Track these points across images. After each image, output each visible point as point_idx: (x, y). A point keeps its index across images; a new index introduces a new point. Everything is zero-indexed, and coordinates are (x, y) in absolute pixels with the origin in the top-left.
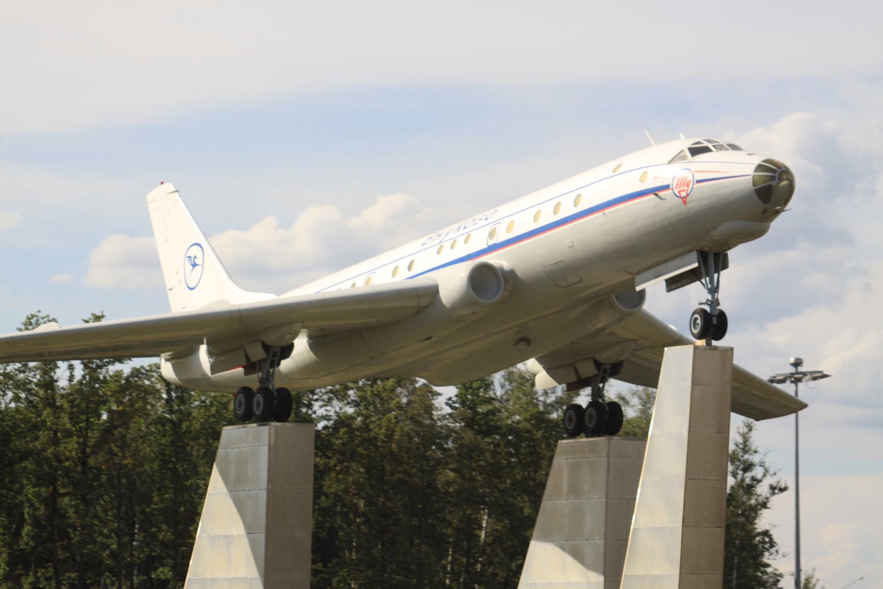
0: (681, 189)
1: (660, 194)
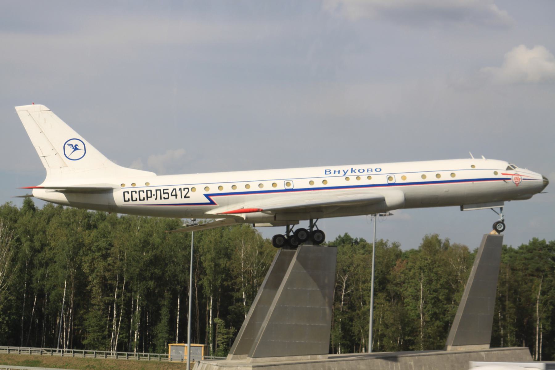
0: (516, 181)
1: (507, 181)
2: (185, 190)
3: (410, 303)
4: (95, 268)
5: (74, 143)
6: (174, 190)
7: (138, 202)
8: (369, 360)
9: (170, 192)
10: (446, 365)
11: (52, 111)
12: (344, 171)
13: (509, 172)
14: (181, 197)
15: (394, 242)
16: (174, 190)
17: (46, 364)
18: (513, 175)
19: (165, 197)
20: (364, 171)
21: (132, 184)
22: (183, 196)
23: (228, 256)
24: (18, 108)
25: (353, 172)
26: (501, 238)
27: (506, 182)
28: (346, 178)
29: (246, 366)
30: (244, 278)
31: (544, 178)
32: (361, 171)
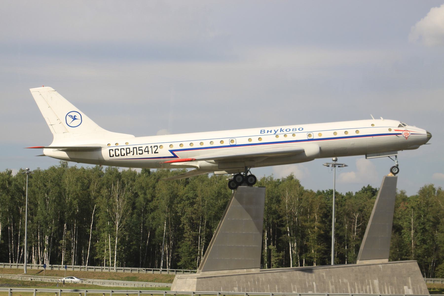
1: (398, 135)
2: (155, 147)
3: (405, 232)
4: (185, 212)
5: (73, 114)
6: (147, 148)
7: (120, 157)
8: (290, 272)
9: (143, 149)
10: (351, 274)
11: (57, 91)
12: (275, 130)
13: (400, 129)
14: (152, 153)
15: (401, 190)
16: (147, 148)
17: (141, 279)
18: (403, 131)
20: (290, 130)
21: (116, 144)
22: (153, 152)
23: (279, 201)
24: (32, 90)
25: (282, 131)
26: (396, 179)
27: (398, 136)
28: (276, 136)
29: (193, 277)
30: (288, 217)
31: (428, 133)
32: (288, 130)
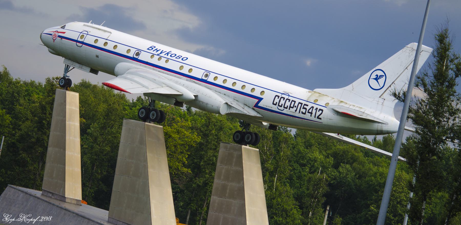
6: (312, 108)
9: (308, 108)
14: (315, 117)
16: (312, 108)
19: (303, 112)
